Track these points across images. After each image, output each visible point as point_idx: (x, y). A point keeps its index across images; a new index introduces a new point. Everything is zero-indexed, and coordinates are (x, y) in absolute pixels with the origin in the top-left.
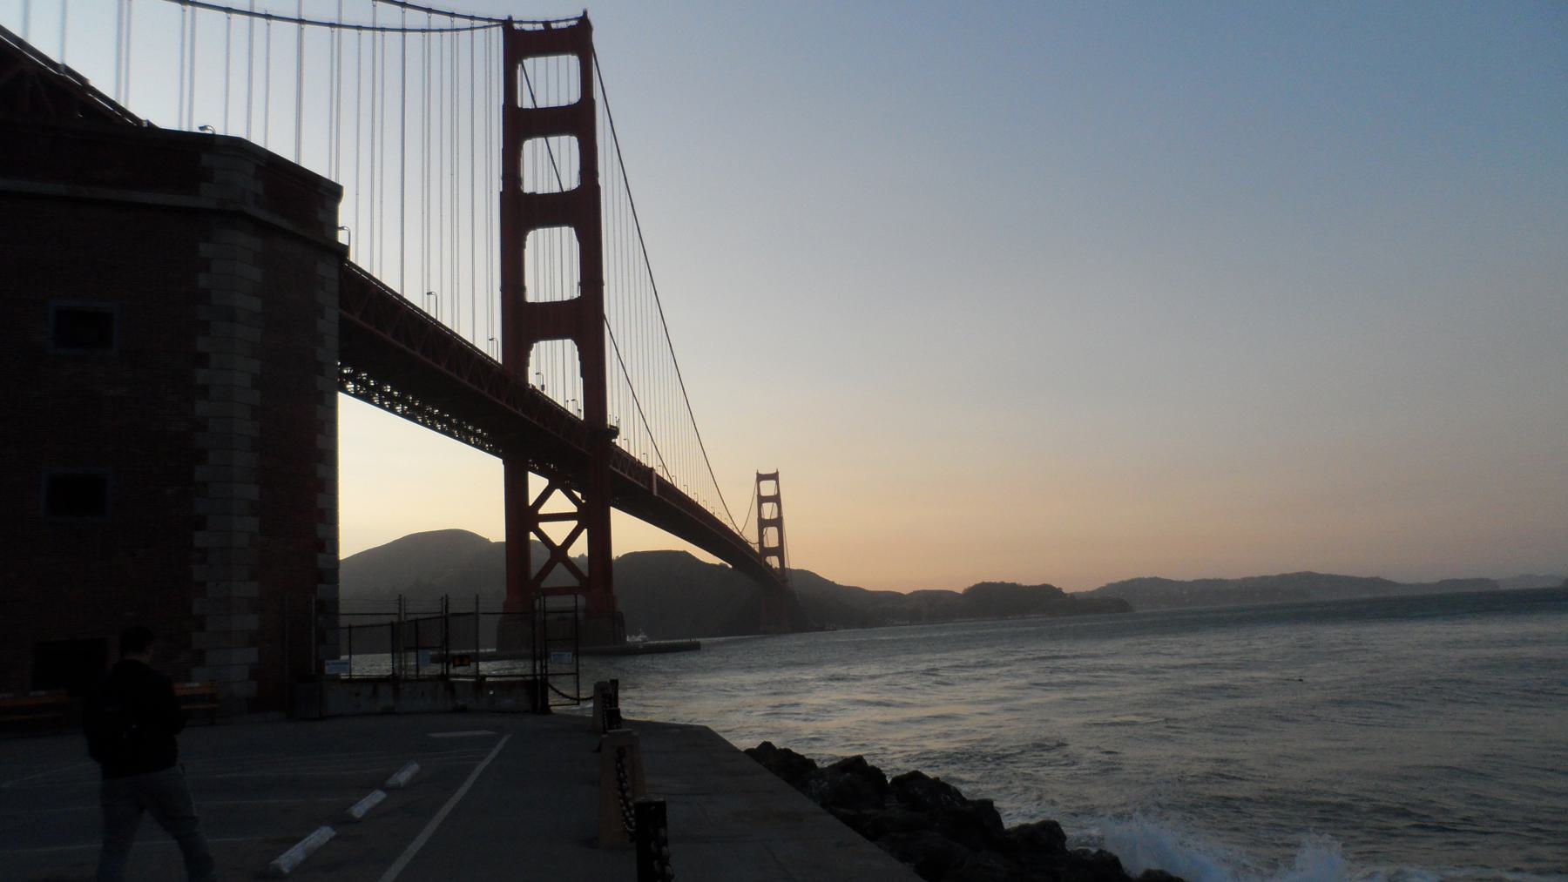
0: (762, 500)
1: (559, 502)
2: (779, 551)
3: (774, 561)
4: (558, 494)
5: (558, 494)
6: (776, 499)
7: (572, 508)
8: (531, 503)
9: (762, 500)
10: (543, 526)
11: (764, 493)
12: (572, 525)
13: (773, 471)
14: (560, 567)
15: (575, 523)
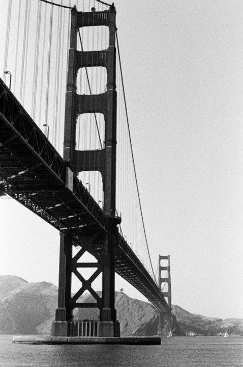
0: (161, 269)
1: (88, 257)
2: (169, 294)
3: (166, 299)
4: (86, 253)
5: (86, 253)
6: (168, 269)
7: (94, 260)
8: (73, 256)
9: (161, 269)
10: (79, 269)
11: (162, 265)
12: (94, 270)
13: (167, 255)
14: (87, 292)
15: (96, 269)
